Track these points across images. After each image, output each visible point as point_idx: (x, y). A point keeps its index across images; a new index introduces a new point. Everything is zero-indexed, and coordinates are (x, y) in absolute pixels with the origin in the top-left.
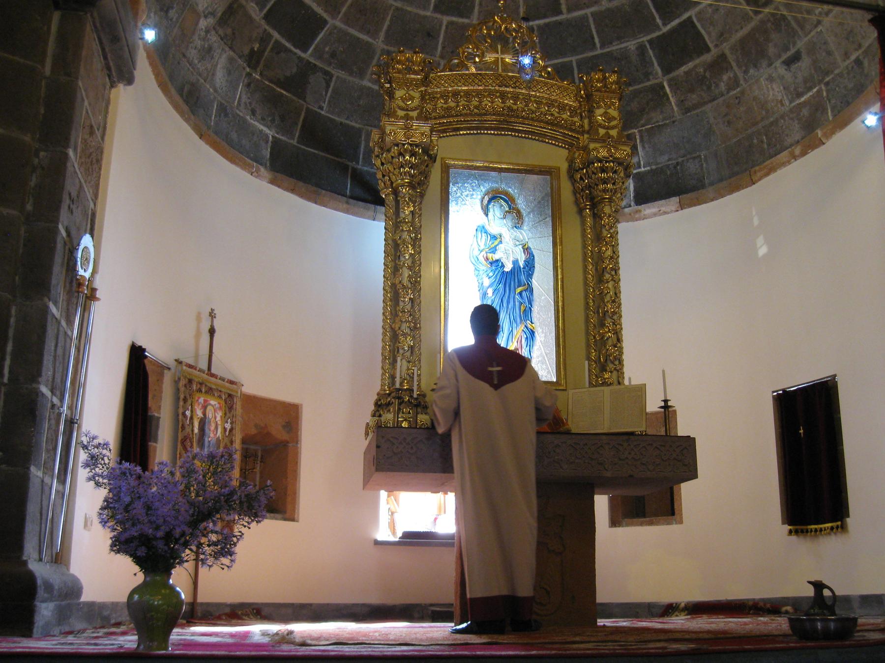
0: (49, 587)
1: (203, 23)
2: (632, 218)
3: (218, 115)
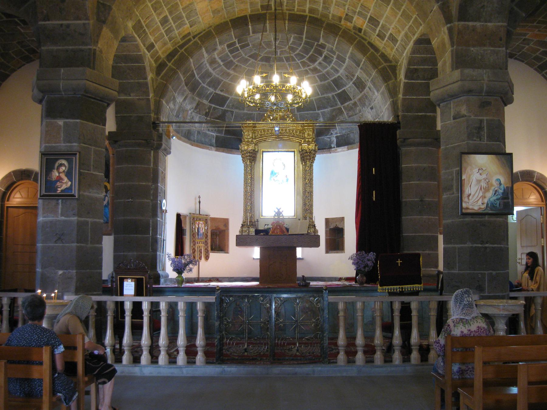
0: (162, 276)
1: (190, 112)
2: (334, 152)
3: (197, 135)
